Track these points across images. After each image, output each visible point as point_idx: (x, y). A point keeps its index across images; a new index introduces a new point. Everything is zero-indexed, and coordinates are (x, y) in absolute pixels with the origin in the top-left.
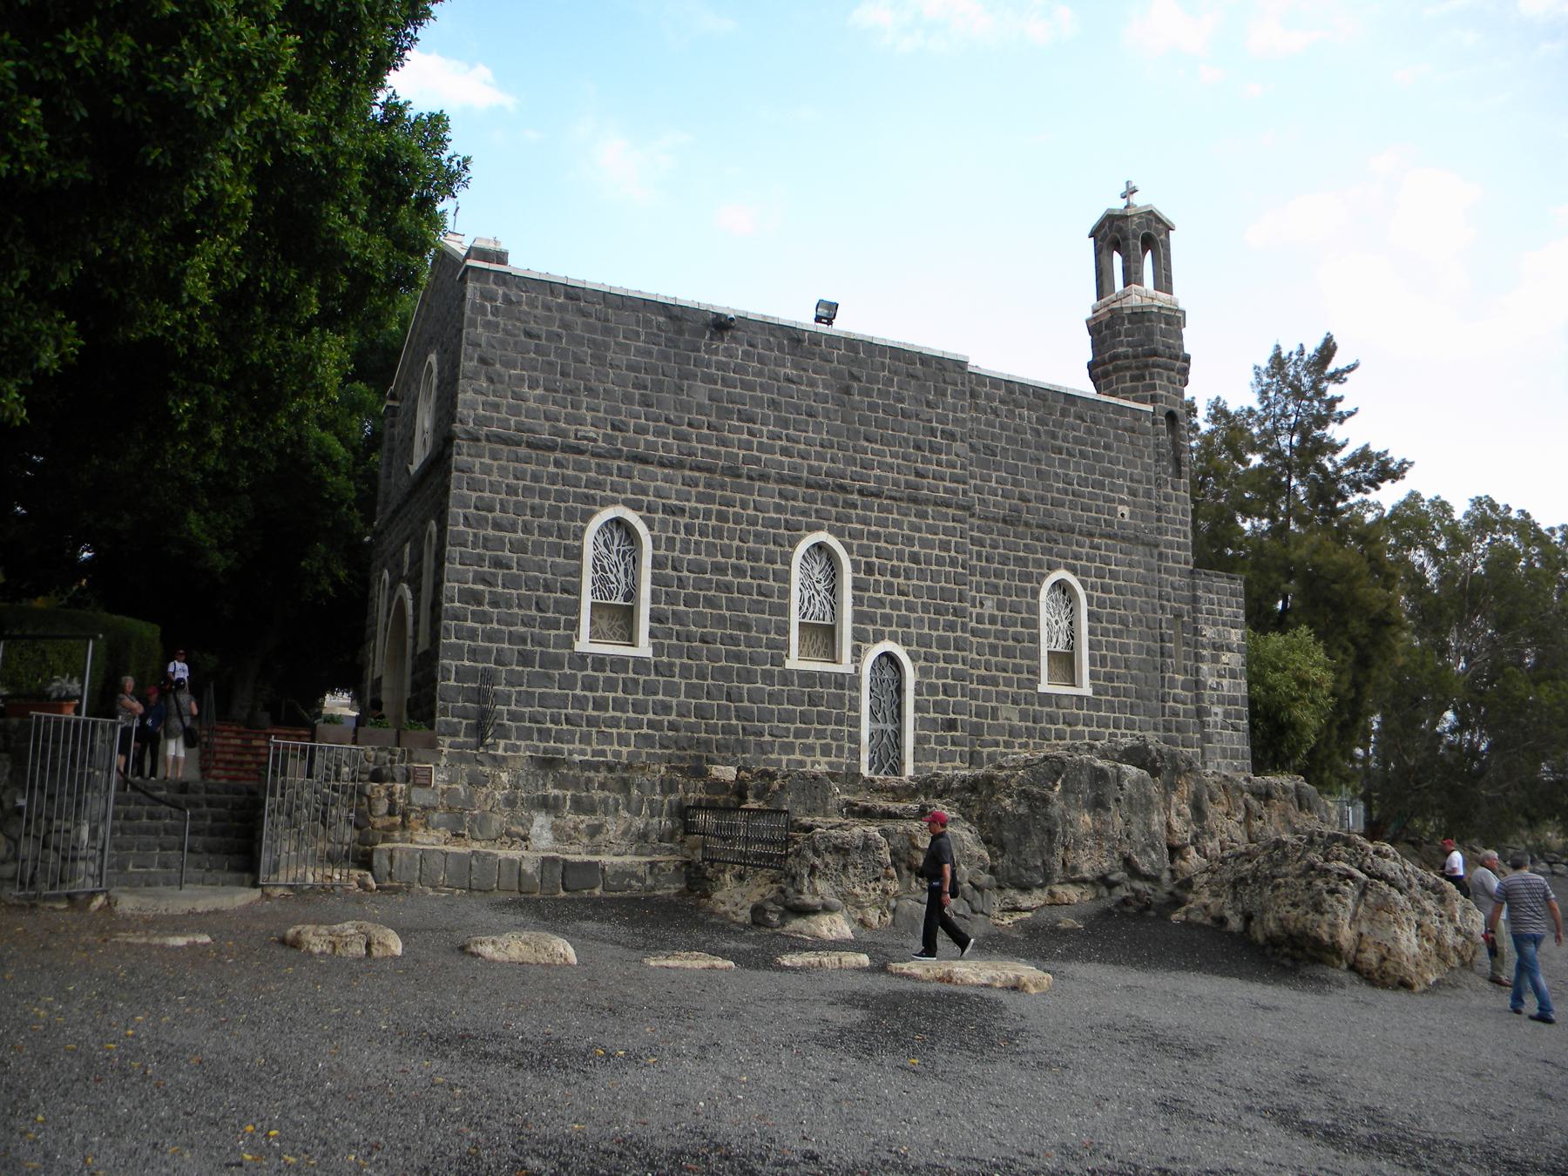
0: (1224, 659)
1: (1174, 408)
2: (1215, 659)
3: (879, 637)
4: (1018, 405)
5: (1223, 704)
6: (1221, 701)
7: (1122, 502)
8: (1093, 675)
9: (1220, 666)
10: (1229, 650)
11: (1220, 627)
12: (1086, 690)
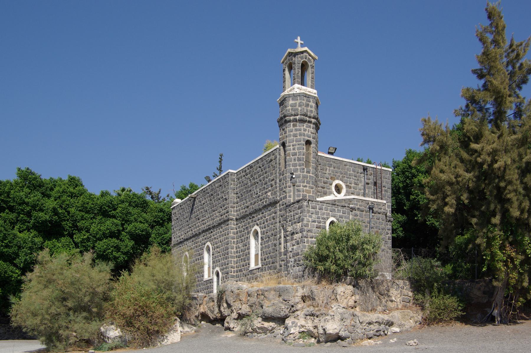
0: (295, 238)
2: (292, 239)
3: (216, 266)
4: (247, 175)
5: (294, 257)
6: (293, 256)
7: (270, 191)
8: (262, 260)
9: (294, 241)
10: (296, 233)
11: (294, 225)
12: (260, 266)
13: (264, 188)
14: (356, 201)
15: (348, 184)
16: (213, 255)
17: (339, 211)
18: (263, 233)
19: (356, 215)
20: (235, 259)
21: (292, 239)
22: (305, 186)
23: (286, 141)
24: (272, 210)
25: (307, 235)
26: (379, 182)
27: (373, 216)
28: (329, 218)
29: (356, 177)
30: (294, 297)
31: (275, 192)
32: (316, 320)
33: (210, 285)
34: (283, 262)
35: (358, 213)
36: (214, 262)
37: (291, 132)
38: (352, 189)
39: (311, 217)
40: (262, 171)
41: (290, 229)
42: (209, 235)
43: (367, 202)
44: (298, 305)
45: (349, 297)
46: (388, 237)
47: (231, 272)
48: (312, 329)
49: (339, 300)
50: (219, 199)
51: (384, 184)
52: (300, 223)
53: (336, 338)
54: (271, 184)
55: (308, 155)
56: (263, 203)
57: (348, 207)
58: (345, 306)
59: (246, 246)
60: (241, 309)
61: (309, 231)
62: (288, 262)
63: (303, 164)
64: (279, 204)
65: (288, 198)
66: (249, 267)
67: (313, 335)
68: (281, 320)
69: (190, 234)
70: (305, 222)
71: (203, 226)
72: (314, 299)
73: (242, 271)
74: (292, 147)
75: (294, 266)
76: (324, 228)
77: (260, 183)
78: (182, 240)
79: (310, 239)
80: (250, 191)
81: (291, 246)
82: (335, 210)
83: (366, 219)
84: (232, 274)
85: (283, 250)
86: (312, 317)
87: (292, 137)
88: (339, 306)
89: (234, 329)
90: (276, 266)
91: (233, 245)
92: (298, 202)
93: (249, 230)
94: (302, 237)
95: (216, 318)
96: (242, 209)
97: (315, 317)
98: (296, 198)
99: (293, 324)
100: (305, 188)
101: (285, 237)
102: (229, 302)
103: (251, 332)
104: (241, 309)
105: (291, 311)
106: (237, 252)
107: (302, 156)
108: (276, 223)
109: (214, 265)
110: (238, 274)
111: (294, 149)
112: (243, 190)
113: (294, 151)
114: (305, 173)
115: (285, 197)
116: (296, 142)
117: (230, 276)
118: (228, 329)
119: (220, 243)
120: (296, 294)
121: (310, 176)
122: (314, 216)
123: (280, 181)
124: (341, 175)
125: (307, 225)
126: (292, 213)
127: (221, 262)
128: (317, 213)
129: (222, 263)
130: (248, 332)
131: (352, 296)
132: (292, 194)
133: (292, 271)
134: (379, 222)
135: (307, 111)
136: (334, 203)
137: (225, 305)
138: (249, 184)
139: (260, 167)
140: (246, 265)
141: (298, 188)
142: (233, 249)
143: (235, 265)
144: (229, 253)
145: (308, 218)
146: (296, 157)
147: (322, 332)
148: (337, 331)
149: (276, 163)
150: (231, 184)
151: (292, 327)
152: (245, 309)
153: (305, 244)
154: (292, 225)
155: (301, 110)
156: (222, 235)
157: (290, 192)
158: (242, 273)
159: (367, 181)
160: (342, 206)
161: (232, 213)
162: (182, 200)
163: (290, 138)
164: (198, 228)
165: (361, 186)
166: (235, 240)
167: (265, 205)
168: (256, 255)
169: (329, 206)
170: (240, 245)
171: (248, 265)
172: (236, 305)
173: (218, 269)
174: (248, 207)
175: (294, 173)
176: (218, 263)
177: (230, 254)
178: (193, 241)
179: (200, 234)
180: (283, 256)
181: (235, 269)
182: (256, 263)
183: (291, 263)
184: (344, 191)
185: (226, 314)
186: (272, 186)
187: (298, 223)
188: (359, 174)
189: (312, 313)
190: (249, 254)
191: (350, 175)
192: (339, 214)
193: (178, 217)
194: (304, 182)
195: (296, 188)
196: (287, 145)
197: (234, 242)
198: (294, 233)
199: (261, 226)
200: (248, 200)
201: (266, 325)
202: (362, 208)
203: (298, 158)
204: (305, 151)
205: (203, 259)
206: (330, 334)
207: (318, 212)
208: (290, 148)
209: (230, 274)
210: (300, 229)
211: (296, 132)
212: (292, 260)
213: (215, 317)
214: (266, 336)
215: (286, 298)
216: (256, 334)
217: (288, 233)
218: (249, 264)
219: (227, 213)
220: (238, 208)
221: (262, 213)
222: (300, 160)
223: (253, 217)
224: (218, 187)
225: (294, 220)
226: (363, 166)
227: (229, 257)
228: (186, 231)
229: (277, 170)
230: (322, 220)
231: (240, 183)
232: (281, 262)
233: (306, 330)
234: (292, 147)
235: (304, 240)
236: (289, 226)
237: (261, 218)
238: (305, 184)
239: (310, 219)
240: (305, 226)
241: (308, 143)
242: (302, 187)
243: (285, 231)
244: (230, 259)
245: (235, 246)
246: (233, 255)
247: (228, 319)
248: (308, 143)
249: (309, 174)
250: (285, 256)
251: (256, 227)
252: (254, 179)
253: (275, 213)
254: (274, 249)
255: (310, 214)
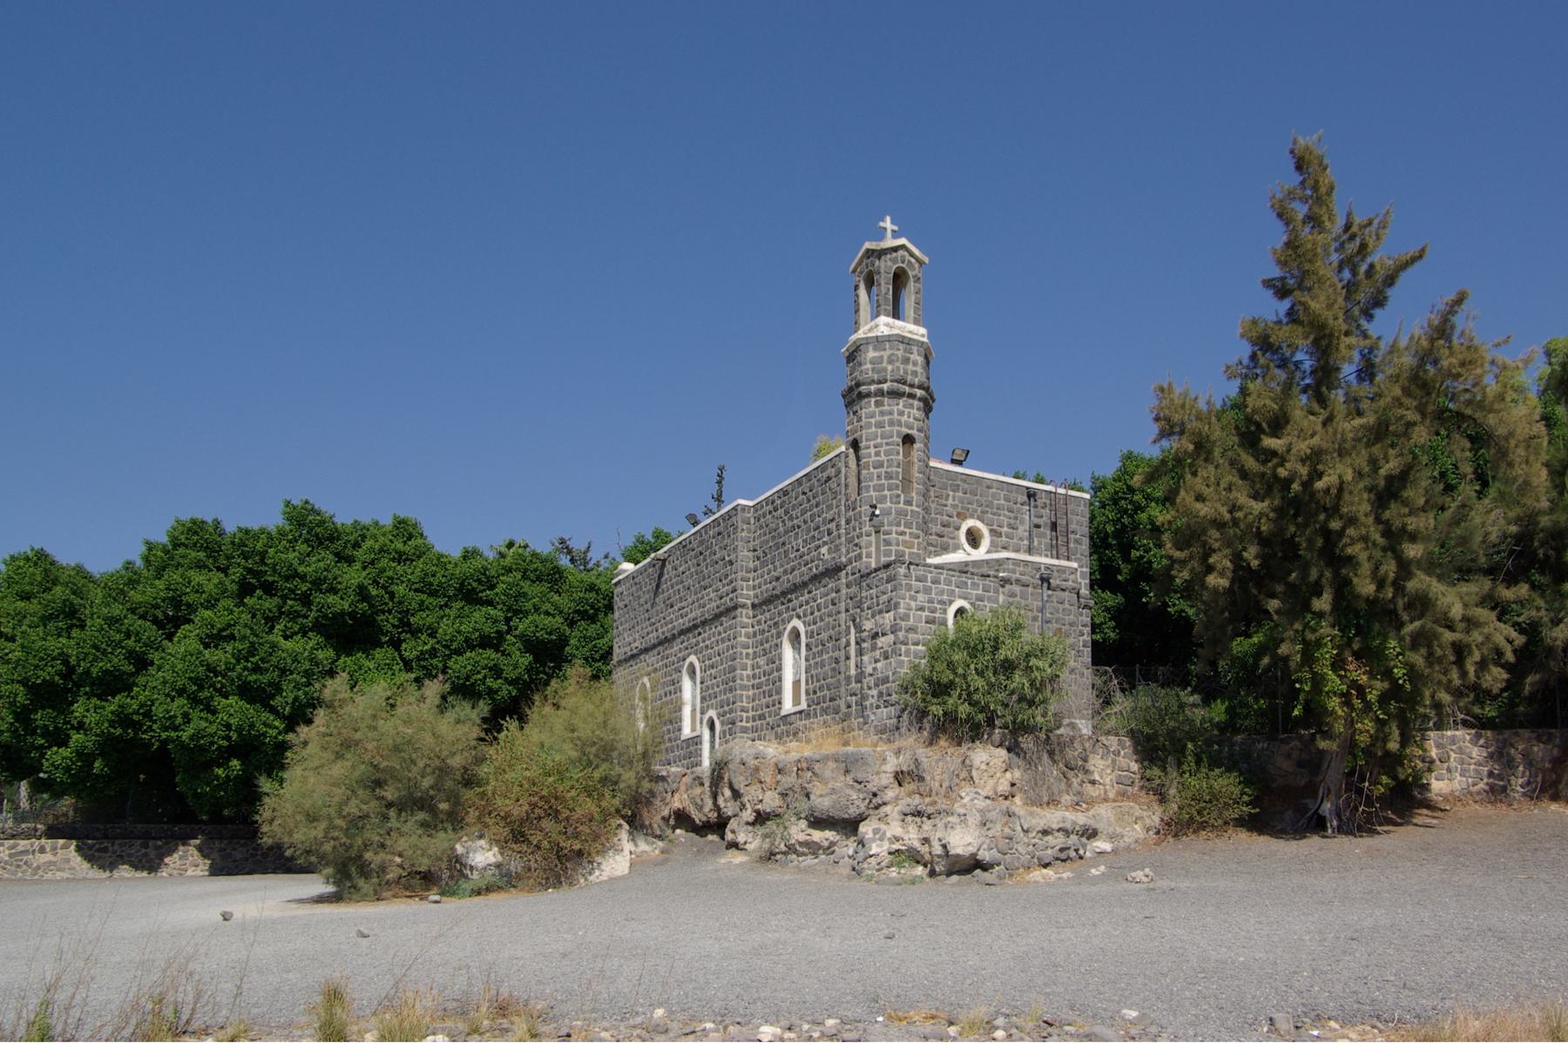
0: (880, 645)
1: (856, 435)
3: (708, 706)
4: (776, 510)
6: (877, 685)
7: (825, 543)
8: (807, 693)
9: (878, 652)
10: (883, 635)
11: (877, 617)
12: (804, 706)
13: (814, 537)
14: (1013, 564)
15: (995, 527)
16: (702, 683)
17: (975, 585)
18: (810, 635)
19: (1013, 595)
20: (751, 693)
21: (874, 648)
22: (902, 533)
23: (861, 436)
24: (830, 586)
25: (907, 637)
26: (1061, 522)
27: (1049, 596)
28: (953, 601)
29: (1012, 512)
30: (878, 773)
31: (837, 546)
32: (928, 825)
33: (696, 750)
34: (854, 698)
35: (1017, 589)
36: (703, 699)
37: (872, 417)
38: (1004, 538)
39: (916, 600)
40: (809, 501)
41: (868, 625)
42: (694, 640)
43: (1037, 567)
44: (886, 791)
45: (998, 775)
46: (1084, 641)
47: (741, 721)
48: (917, 844)
49: (977, 781)
50: (717, 563)
51: (1072, 527)
52: (892, 613)
53: (971, 865)
54: (828, 530)
55: (908, 466)
56: (810, 569)
57: (996, 577)
58: (991, 794)
59: (774, 662)
60: (761, 801)
61: (910, 629)
62: (864, 697)
63: (897, 487)
64: (844, 572)
65: (864, 559)
66: (780, 709)
67: (919, 858)
68: (850, 826)
69: (652, 638)
70: (901, 610)
71: (681, 621)
72: (921, 779)
73: (765, 719)
74: (872, 451)
75: (878, 707)
76: (944, 623)
77: (804, 527)
78: (635, 651)
79: (912, 647)
80: (784, 544)
81: (870, 663)
82: (966, 583)
83: (1035, 603)
84: (744, 724)
85: (853, 672)
86: (918, 819)
87: (874, 429)
88: (976, 793)
89: (747, 846)
90: (839, 706)
91: (745, 661)
92: (887, 566)
93: (781, 628)
94: (895, 643)
95: (708, 822)
96: (766, 584)
97: (925, 819)
98: (883, 559)
99: (875, 834)
100: (901, 538)
101: (857, 643)
102: (736, 787)
103: (784, 853)
104: (761, 801)
105: (872, 806)
106: (754, 677)
107: (894, 469)
108: (839, 612)
109: (705, 705)
110: (757, 725)
111: (877, 454)
112: (767, 542)
113: (878, 458)
114: (901, 505)
115: (859, 557)
116: (882, 438)
117: (738, 730)
118: (734, 845)
119: (718, 658)
120: (884, 768)
121: (912, 511)
122: (920, 597)
123: (848, 522)
124: (979, 509)
125: (906, 617)
126: (873, 591)
127: (719, 699)
128: (927, 591)
129: (721, 701)
130: (778, 853)
131: (1006, 770)
132: (873, 549)
133: (872, 717)
134: (1064, 610)
135: (906, 372)
136: (963, 569)
137: (728, 793)
138: (781, 529)
139: (804, 493)
140: (774, 705)
141: (886, 537)
142: (746, 670)
143: (751, 705)
144: (738, 677)
145: (907, 600)
146: (883, 470)
147: (939, 853)
148: (972, 849)
149: (839, 485)
150: (743, 530)
151: (873, 840)
152: (771, 801)
153: (902, 658)
154: (873, 616)
155: (893, 371)
156: (723, 640)
157: (869, 545)
158: (764, 722)
159: (1036, 521)
160: (982, 576)
161: (745, 592)
162: (636, 564)
163: (869, 431)
164: (670, 626)
165: (1022, 531)
166: (750, 651)
167: (816, 575)
168: (796, 683)
169: (953, 576)
170: (762, 661)
171: (777, 706)
172: (751, 793)
173: (712, 713)
174: (778, 579)
175: (878, 506)
176: (713, 701)
177: (738, 681)
178: (659, 654)
179: (674, 637)
180: (853, 685)
181: (751, 714)
182: (796, 701)
183: (871, 700)
184: (986, 543)
185: (730, 814)
186: (829, 534)
187: (887, 612)
188: (1019, 506)
189: (919, 808)
190: (780, 679)
191: (998, 509)
192: (975, 592)
193: (627, 602)
194: (898, 524)
195: (882, 537)
196: (862, 445)
197: (747, 654)
198: (877, 634)
199: (807, 619)
200: (777, 564)
201: (818, 836)
202: (1025, 578)
203: (886, 472)
204: (901, 457)
205: (681, 691)
206: (958, 856)
207: (931, 588)
208: (869, 452)
209: (740, 724)
210: (891, 626)
211: (881, 418)
212: (874, 692)
213: (704, 819)
214: (816, 861)
215: (860, 777)
216: (794, 856)
217: (866, 634)
218: (780, 703)
219: (732, 592)
220: (757, 582)
221: (809, 592)
222: (891, 478)
223: (790, 601)
224: (714, 537)
225: (878, 605)
226: (1027, 488)
227: (738, 687)
228: (645, 631)
229: (840, 500)
230: (939, 606)
231: (761, 527)
232: (849, 698)
233: (903, 848)
234: (872, 451)
235: (900, 649)
236: (868, 619)
237: (807, 603)
238: (902, 528)
239: (913, 604)
240: (902, 619)
241: (908, 440)
242: (894, 535)
243: (859, 630)
244: (739, 692)
245: (749, 662)
246: (745, 682)
247: (733, 824)
248: (908, 440)
249: (909, 508)
250: (859, 685)
251: (796, 623)
252: (791, 518)
253: (838, 591)
254: (833, 669)
255: (913, 593)
